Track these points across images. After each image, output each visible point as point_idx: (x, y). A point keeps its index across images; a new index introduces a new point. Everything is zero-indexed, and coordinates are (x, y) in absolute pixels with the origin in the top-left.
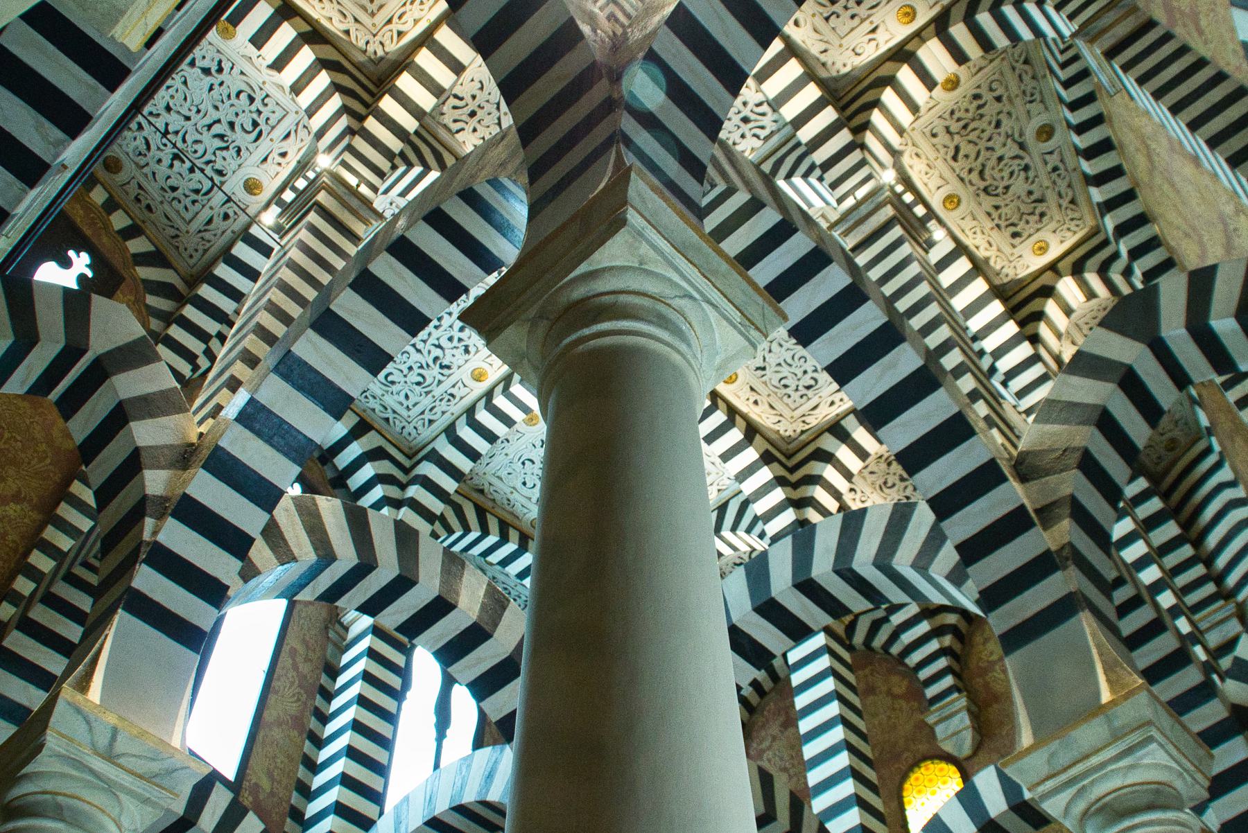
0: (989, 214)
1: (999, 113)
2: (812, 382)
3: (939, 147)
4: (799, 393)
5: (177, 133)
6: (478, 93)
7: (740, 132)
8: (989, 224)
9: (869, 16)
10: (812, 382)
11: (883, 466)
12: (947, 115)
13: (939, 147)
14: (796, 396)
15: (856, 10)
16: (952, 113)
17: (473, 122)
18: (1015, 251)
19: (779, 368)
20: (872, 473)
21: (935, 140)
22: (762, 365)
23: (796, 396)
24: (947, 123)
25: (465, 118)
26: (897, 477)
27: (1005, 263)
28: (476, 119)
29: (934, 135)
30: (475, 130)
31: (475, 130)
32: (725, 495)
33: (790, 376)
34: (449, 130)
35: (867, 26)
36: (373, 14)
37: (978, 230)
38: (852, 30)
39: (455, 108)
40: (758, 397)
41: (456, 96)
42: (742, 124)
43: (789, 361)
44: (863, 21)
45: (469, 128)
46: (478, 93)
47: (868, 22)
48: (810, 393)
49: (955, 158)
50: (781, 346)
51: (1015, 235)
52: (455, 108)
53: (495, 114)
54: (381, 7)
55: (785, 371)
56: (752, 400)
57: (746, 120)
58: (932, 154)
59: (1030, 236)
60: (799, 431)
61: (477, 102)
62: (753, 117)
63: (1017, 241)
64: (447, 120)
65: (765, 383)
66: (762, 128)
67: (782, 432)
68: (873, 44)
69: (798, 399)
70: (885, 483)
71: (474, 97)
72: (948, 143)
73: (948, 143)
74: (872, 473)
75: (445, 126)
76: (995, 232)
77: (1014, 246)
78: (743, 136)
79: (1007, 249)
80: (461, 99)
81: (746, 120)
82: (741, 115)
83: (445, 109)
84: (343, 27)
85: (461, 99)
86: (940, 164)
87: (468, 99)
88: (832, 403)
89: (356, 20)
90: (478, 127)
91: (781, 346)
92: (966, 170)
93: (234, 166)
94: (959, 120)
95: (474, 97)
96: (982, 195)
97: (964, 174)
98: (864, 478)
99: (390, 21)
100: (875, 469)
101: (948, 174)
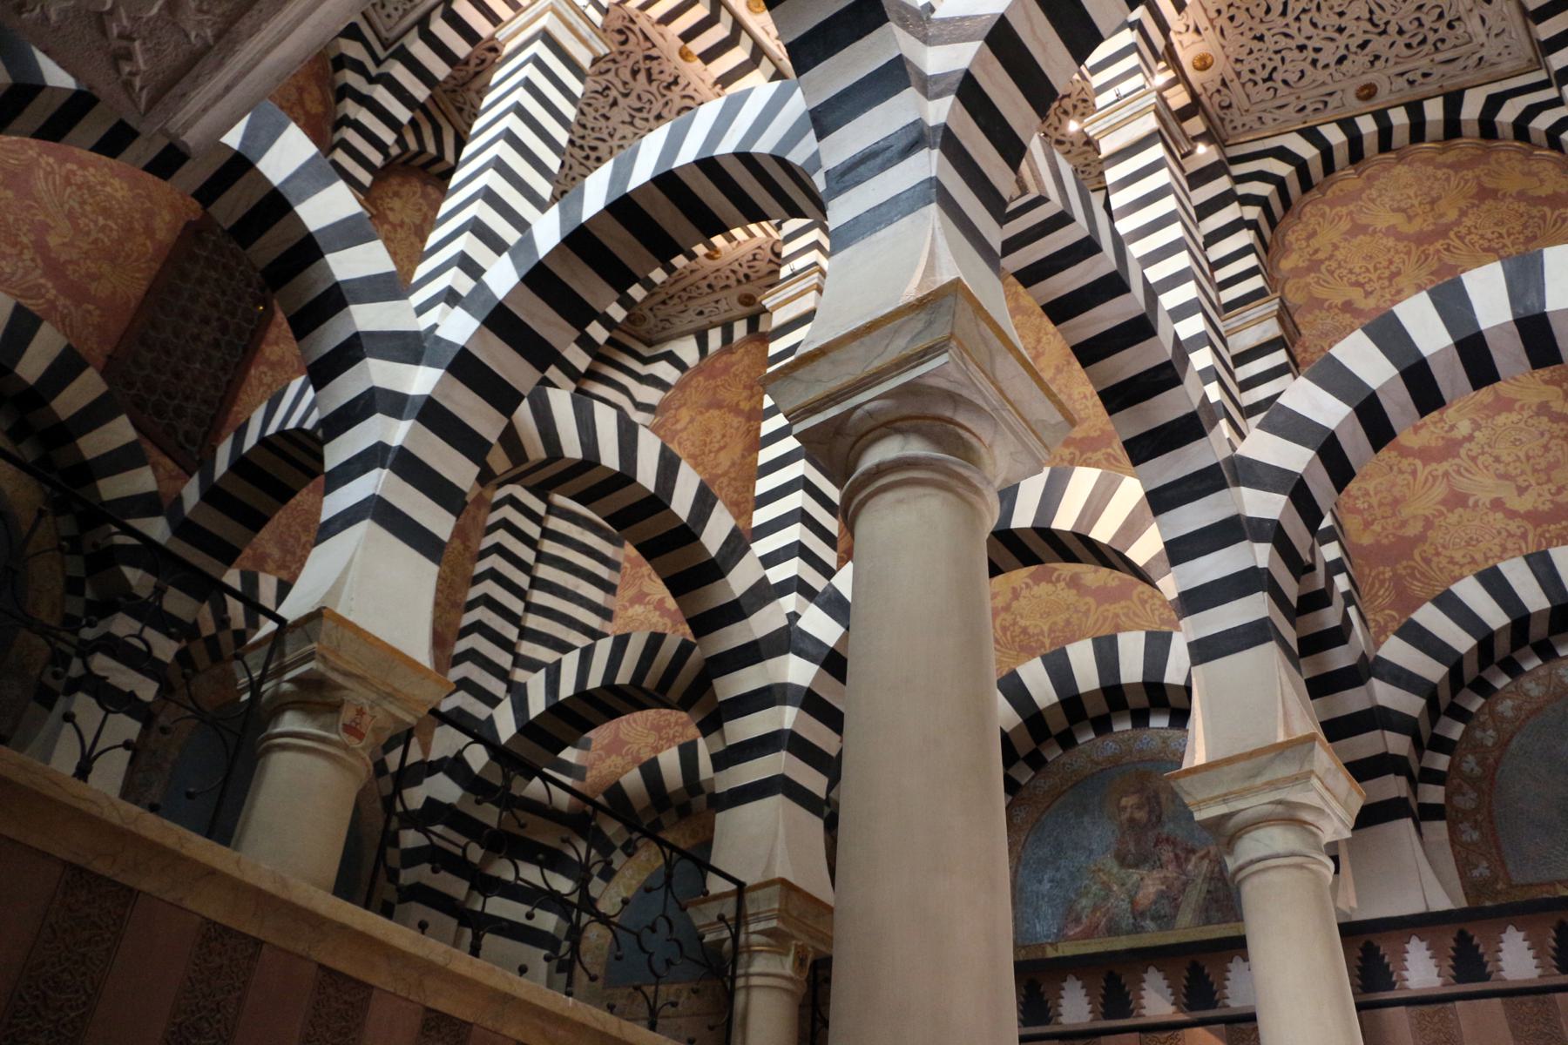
1: (1072, 144)
9: (1214, 28)
11: (618, 25)
12: (1083, 96)
15: (1225, 15)
16: (1085, 101)
24: (1074, 97)
35: (1203, 24)
38: (1205, 10)
44: (1211, 21)
47: (1207, 24)
68: (1183, 29)
94: (1075, 107)
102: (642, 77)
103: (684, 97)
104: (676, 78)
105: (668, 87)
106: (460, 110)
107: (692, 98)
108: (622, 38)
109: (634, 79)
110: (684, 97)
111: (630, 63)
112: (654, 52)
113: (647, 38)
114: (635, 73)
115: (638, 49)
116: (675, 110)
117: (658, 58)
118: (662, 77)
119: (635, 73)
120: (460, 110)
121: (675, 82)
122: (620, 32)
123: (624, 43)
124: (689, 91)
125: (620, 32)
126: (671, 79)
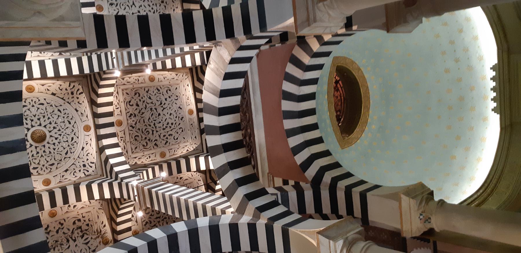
5: (132, 6)
17: (70, 92)
25: (73, 90)
28: (70, 93)
30: (66, 89)
31: (66, 89)
34: (73, 82)
36: (123, 90)
39: (78, 90)
41: (82, 93)
45: (68, 89)
46: (78, 100)
52: (78, 90)
53: (67, 100)
54: (123, 94)
61: (75, 98)
64: (76, 84)
71: (78, 98)
75: (75, 82)
83: (80, 87)
84: (125, 79)
85: (80, 94)
89: (124, 84)
90: (66, 92)
93: (110, 10)
99: (118, 93)
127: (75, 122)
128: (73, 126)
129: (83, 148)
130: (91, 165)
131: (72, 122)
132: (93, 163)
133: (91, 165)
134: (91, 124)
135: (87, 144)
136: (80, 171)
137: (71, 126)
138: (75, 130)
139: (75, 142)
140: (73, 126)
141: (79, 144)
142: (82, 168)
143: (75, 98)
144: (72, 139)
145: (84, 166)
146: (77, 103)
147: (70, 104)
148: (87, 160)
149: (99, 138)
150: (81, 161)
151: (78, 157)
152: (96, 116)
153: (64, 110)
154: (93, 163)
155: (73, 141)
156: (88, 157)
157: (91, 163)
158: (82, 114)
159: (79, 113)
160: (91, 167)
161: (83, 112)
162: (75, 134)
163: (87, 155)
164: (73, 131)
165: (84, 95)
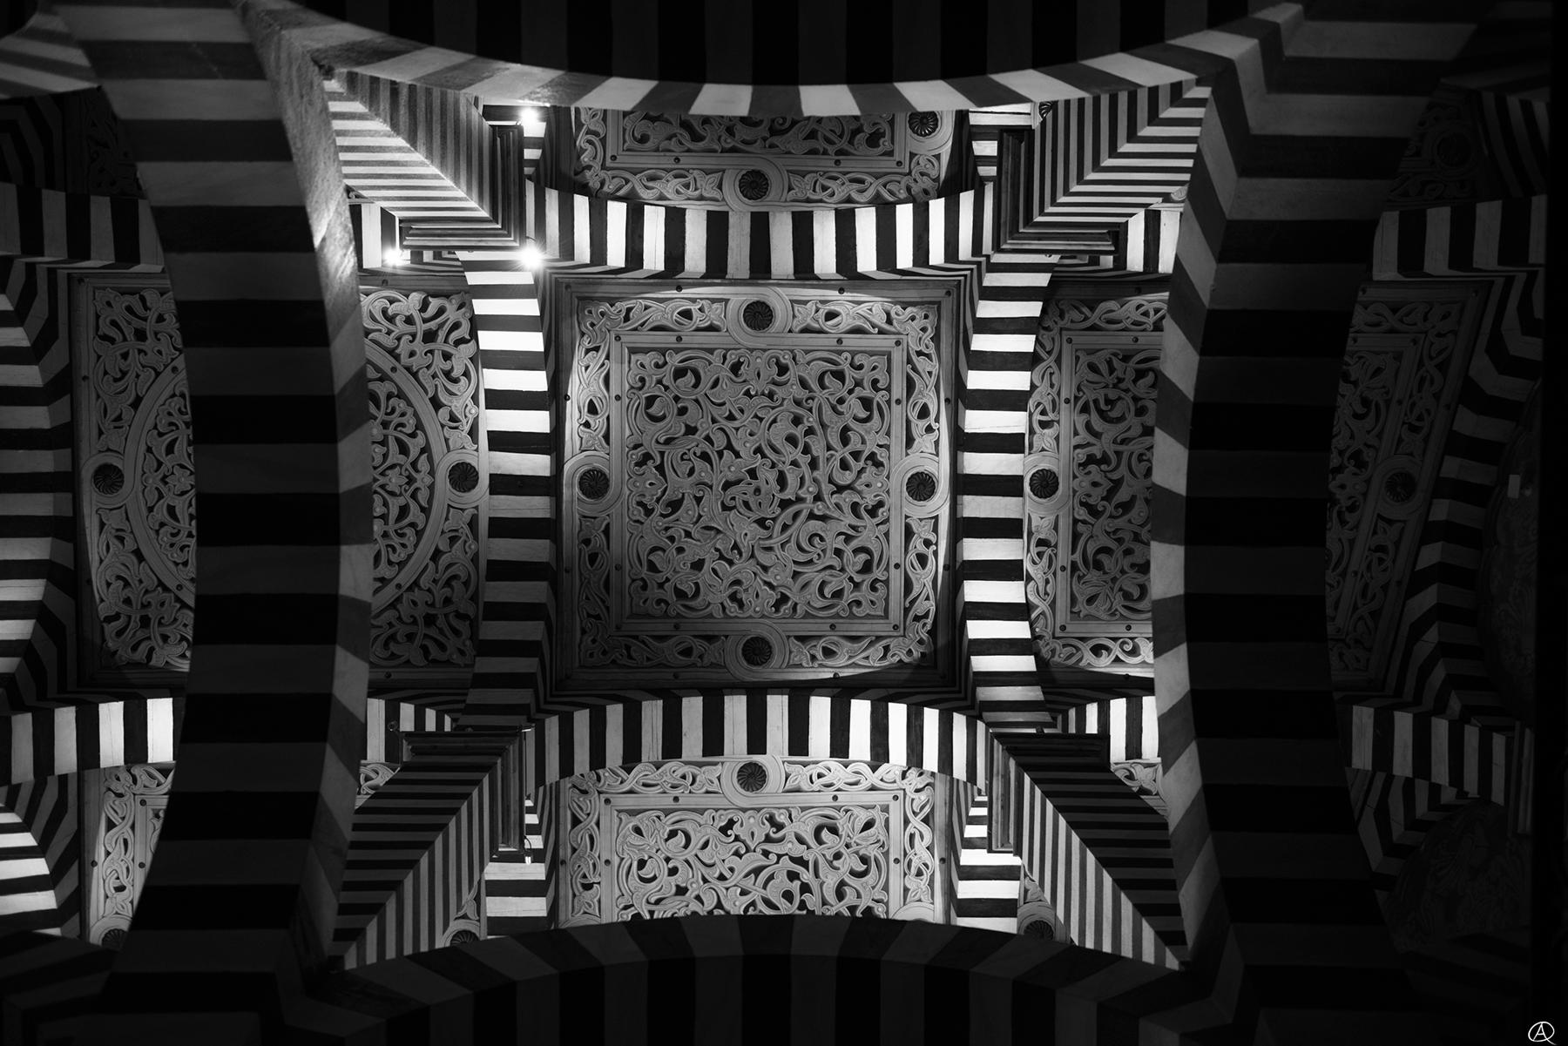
0: (813, 152)
2: (863, 557)
3: (665, 144)
4: (865, 586)
6: (127, 593)
7: (438, 355)
8: (827, 163)
10: (863, 557)
11: (1094, 575)
13: (665, 144)
14: (864, 594)
17: (155, 631)
18: (897, 157)
19: (801, 580)
20: (1090, 601)
21: (649, 145)
22: (775, 596)
23: (864, 594)
25: (140, 635)
26: (1132, 573)
27: (904, 180)
28: (154, 623)
29: (643, 139)
30: (165, 638)
31: (165, 638)
32: (940, 818)
33: (825, 575)
34: (137, 665)
37: (822, 181)
40: (822, 643)
41: (109, 619)
42: (431, 346)
43: (802, 558)
46: (127, 593)
48: (878, 573)
49: (696, 138)
50: (770, 549)
51: (873, 140)
52: (120, 633)
53: (168, 597)
55: (813, 575)
56: (820, 655)
57: (430, 337)
58: (667, 161)
59: (892, 123)
60: (925, 636)
61: (136, 604)
62: (432, 325)
63: (885, 143)
64: (125, 654)
65: (807, 615)
66: (456, 326)
67: (906, 660)
69: (872, 596)
70: (1127, 596)
72: (670, 130)
73: (670, 130)
74: (1090, 601)
76: (847, 164)
77: (890, 153)
78: (447, 357)
79: (887, 165)
80: (117, 617)
81: (430, 337)
82: (419, 336)
85: (117, 617)
86: (686, 161)
87: (125, 609)
88: (922, 559)
90: (167, 631)
91: (770, 549)
92: (725, 136)
95: (127, 601)
96: (776, 140)
97: (730, 143)
98: (1089, 617)
100: (1090, 591)
101: (710, 162)
102: (1123, 495)
103: (1097, 435)
104: (1083, 465)
105: (1105, 460)
106: (1375, 615)
107: (1088, 427)
108: (1102, 557)
109: (1134, 498)
110: (1097, 435)
111: (1120, 522)
112: (1082, 514)
113: (1076, 537)
114: (1126, 507)
115: (1097, 530)
116: (1122, 426)
117: (1082, 504)
118: (1098, 478)
119: (1126, 507)
120: (1375, 615)
121: (1091, 459)
122: (1098, 566)
123: (1106, 550)
124: (1084, 436)
125: (1098, 566)
126: (1093, 468)
127: (151, 509)
128: (161, 496)
129: (136, 404)
130: (113, 332)
131: (161, 513)
132: (105, 338)
133: (113, 332)
134: (91, 499)
135: (119, 418)
136: (160, 319)
137: (169, 499)
138: (154, 480)
139: (161, 435)
140: (161, 496)
141: (150, 423)
142: (150, 326)
143: (136, 604)
144: (170, 449)
145: (141, 335)
146: (134, 582)
147: (161, 584)
148: (125, 356)
149: (63, 437)
150: (152, 358)
151: (158, 374)
152: (66, 529)
153: (185, 564)
154: (105, 338)
155: (168, 438)
156: (123, 365)
157: (112, 340)
158: (121, 539)
159: (130, 544)
160: (114, 323)
161: (114, 543)
162: (160, 464)
163: (124, 374)
164: (164, 480)
165: (103, 610)
